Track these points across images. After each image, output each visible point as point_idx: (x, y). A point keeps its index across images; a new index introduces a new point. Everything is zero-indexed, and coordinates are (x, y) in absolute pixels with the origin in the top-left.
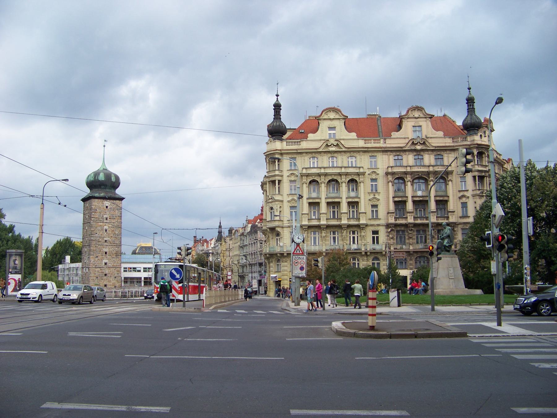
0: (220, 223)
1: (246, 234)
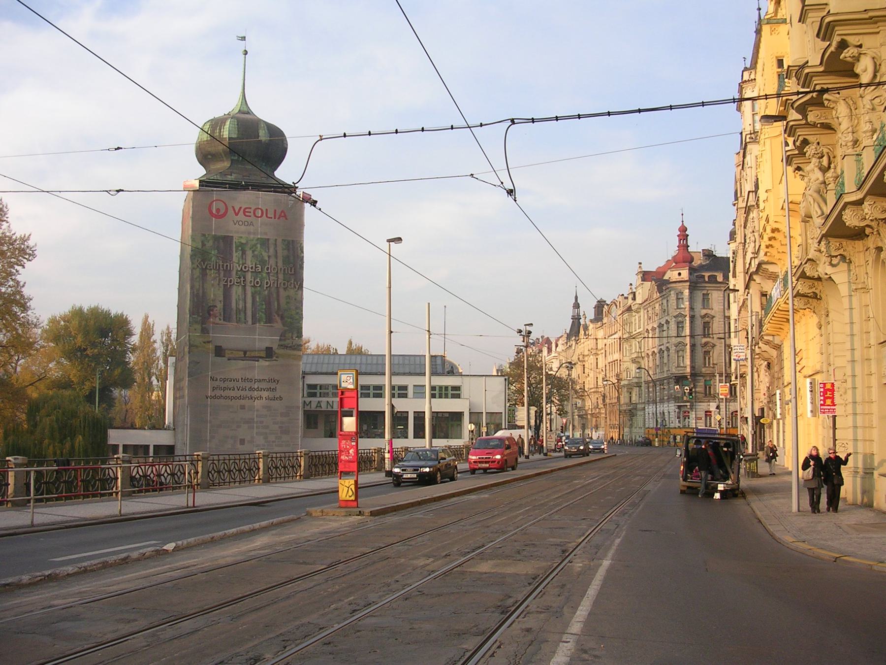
0: (576, 298)
1: (637, 306)
